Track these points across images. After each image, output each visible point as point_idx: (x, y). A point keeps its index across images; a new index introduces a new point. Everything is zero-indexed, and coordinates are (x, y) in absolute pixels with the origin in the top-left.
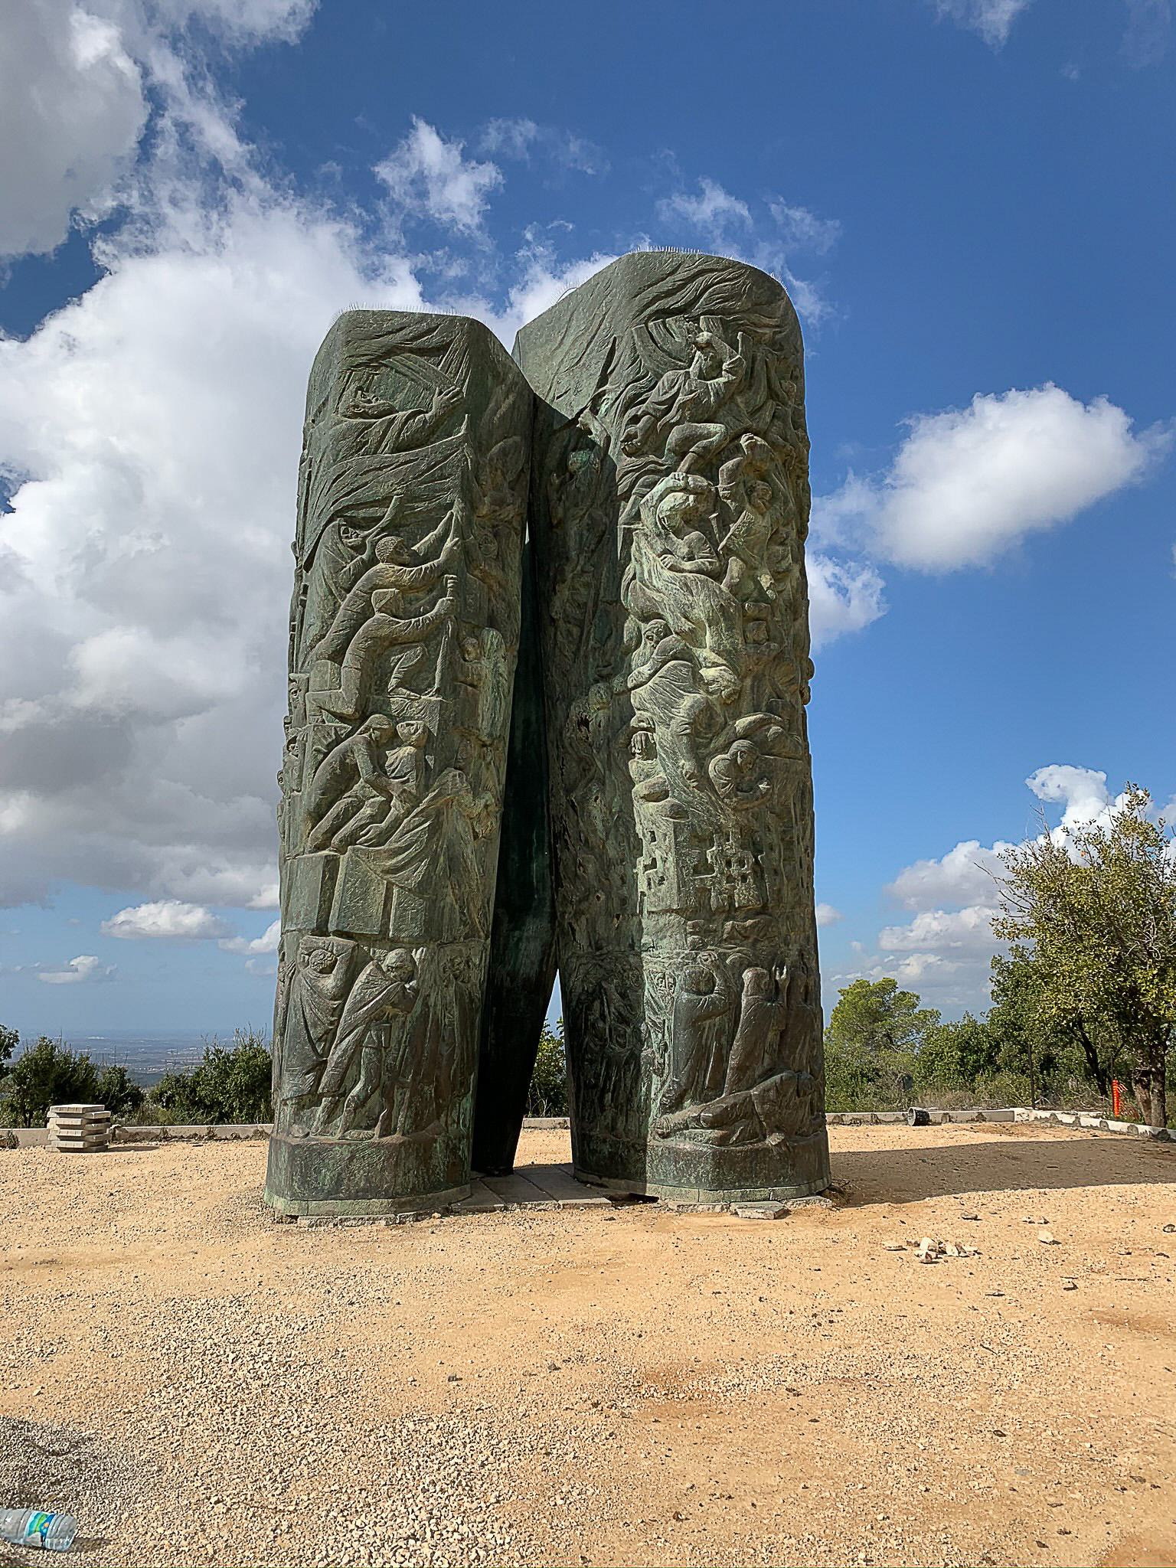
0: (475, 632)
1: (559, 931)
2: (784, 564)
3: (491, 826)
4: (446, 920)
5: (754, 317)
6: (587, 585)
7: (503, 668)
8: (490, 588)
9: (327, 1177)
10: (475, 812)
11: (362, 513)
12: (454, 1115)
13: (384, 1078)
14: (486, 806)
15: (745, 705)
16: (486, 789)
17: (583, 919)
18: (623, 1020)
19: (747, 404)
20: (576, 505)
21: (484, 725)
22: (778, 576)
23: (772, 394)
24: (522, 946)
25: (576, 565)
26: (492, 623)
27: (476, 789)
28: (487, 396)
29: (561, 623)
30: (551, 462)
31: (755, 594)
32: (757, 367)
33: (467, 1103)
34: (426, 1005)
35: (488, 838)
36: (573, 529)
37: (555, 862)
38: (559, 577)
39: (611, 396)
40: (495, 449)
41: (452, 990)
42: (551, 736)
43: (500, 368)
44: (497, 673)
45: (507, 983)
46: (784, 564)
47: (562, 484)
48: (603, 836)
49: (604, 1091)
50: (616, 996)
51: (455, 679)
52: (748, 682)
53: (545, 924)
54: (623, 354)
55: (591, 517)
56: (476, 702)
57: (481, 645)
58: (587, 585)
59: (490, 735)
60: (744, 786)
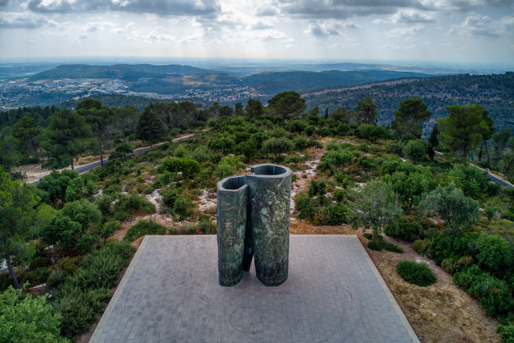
7: (243, 228)
38: (252, 212)
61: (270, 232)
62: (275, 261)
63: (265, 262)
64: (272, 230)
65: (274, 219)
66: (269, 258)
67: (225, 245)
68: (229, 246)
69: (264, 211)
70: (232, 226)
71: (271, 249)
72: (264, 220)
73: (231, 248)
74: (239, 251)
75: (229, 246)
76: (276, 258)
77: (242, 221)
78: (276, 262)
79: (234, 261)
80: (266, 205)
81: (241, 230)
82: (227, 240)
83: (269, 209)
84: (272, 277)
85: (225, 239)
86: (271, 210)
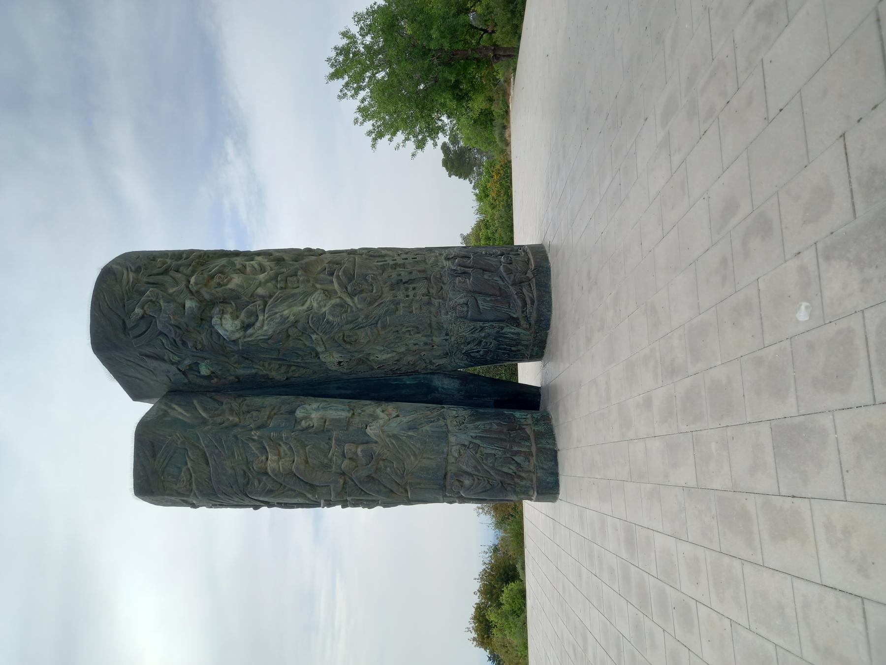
0: (297, 421)
1: (440, 371)
2: (256, 266)
3: (391, 408)
4: (437, 429)
5: (124, 283)
6: (270, 364)
7: (315, 406)
8: (275, 414)
9: (550, 479)
10: (387, 418)
11: (241, 480)
12: (522, 421)
13: (508, 455)
14: (383, 411)
15: (329, 287)
16: (374, 412)
17: (434, 361)
18: (480, 342)
19: (173, 287)
20: (229, 371)
21: (345, 414)
22: (263, 270)
23: (166, 272)
24: (445, 387)
25: (259, 369)
26: (292, 412)
27: (375, 418)
28: (176, 420)
29: (289, 375)
30: (205, 383)
31: (274, 282)
32: (151, 280)
33: (517, 414)
34: (476, 437)
35: (397, 408)
36: (241, 372)
37: (406, 374)
38: (266, 377)
39: (171, 355)
40: (204, 414)
41: (468, 425)
42: (345, 377)
43: (160, 413)
44: (318, 409)
45: (463, 393)
46: (256, 266)
47: (217, 377)
48: (394, 354)
49: (511, 351)
50: (469, 346)
51: (323, 431)
52: (318, 286)
53: (435, 377)
54: (149, 350)
55: (235, 363)
56: (333, 419)
57: (305, 418)
58: (270, 364)
59: (349, 411)
60: (370, 288)
61: (314, 301)
62: (440, 280)
63: (443, 317)
64: (307, 295)
65: (261, 291)
66: (429, 303)
67: (363, 473)
68: (370, 456)
69: (227, 325)
70: (284, 448)
71: (388, 297)
72: (265, 327)
73: (376, 449)
74: (405, 420)
75: (370, 456)
76: (427, 279)
77: (284, 408)
78: (446, 279)
79: (443, 436)
80: (203, 319)
81: (314, 412)
82: (346, 464)
83: (216, 310)
84: (513, 290)
85: (343, 474)
86: (225, 301)
